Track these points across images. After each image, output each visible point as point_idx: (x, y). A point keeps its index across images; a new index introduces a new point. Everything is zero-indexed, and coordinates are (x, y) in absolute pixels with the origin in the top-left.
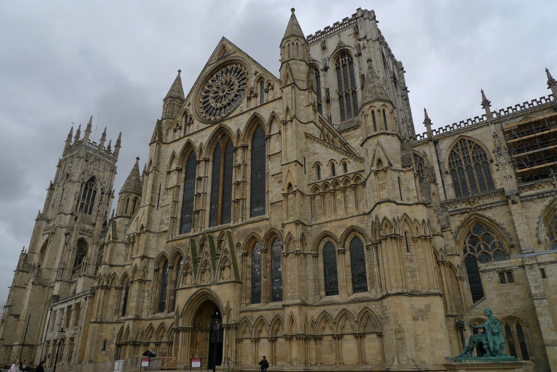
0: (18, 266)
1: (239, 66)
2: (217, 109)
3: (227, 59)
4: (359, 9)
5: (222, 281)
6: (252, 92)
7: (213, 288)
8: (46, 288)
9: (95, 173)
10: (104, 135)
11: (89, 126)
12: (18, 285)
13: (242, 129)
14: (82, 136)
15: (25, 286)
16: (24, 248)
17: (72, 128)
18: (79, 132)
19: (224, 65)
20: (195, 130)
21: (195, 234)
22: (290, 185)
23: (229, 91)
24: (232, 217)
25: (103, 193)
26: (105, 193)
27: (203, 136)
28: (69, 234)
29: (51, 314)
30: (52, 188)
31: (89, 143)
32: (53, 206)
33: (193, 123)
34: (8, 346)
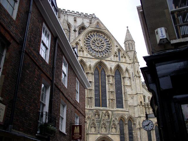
1: (106, 37)
2: (95, 51)
3: (101, 30)
4: (94, 14)
5: (113, 133)
6: (116, 53)
7: (109, 136)
13: (113, 68)
19: (98, 32)
20: (85, 56)
21: (89, 108)
22: (141, 102)
23: (100, 46)
24: (108, 105)
27: (90, 61)
33: (83, 51)
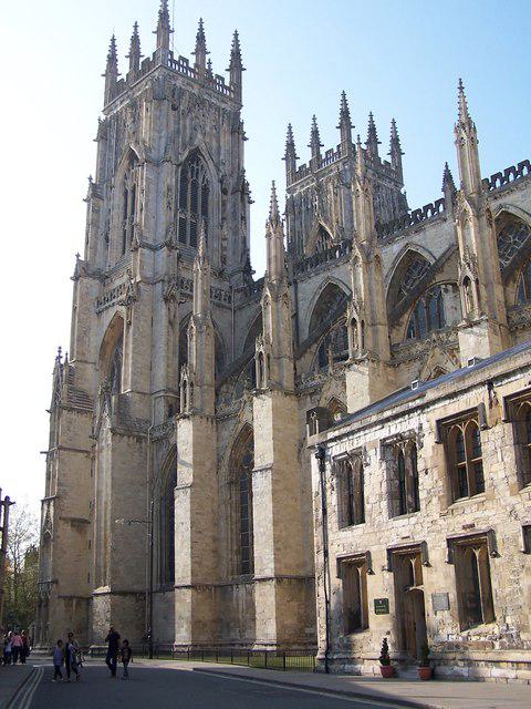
0: (56, 397)
8: (143, 445)
9: (199, 140)
10: (201, 38)
11: (164, 16)
12: (65, 445)
14: (148, 48)
15: (85, 444)
16: (60, 352)
17: (113, 40)
18: (135, 40)
25: (224, 192)
26: (230, 191)
28: (173, 297)
29: (322, 469)
30: (96, 193)
31: (172, 61)
32: (107, 240)
34: (71, 598)
